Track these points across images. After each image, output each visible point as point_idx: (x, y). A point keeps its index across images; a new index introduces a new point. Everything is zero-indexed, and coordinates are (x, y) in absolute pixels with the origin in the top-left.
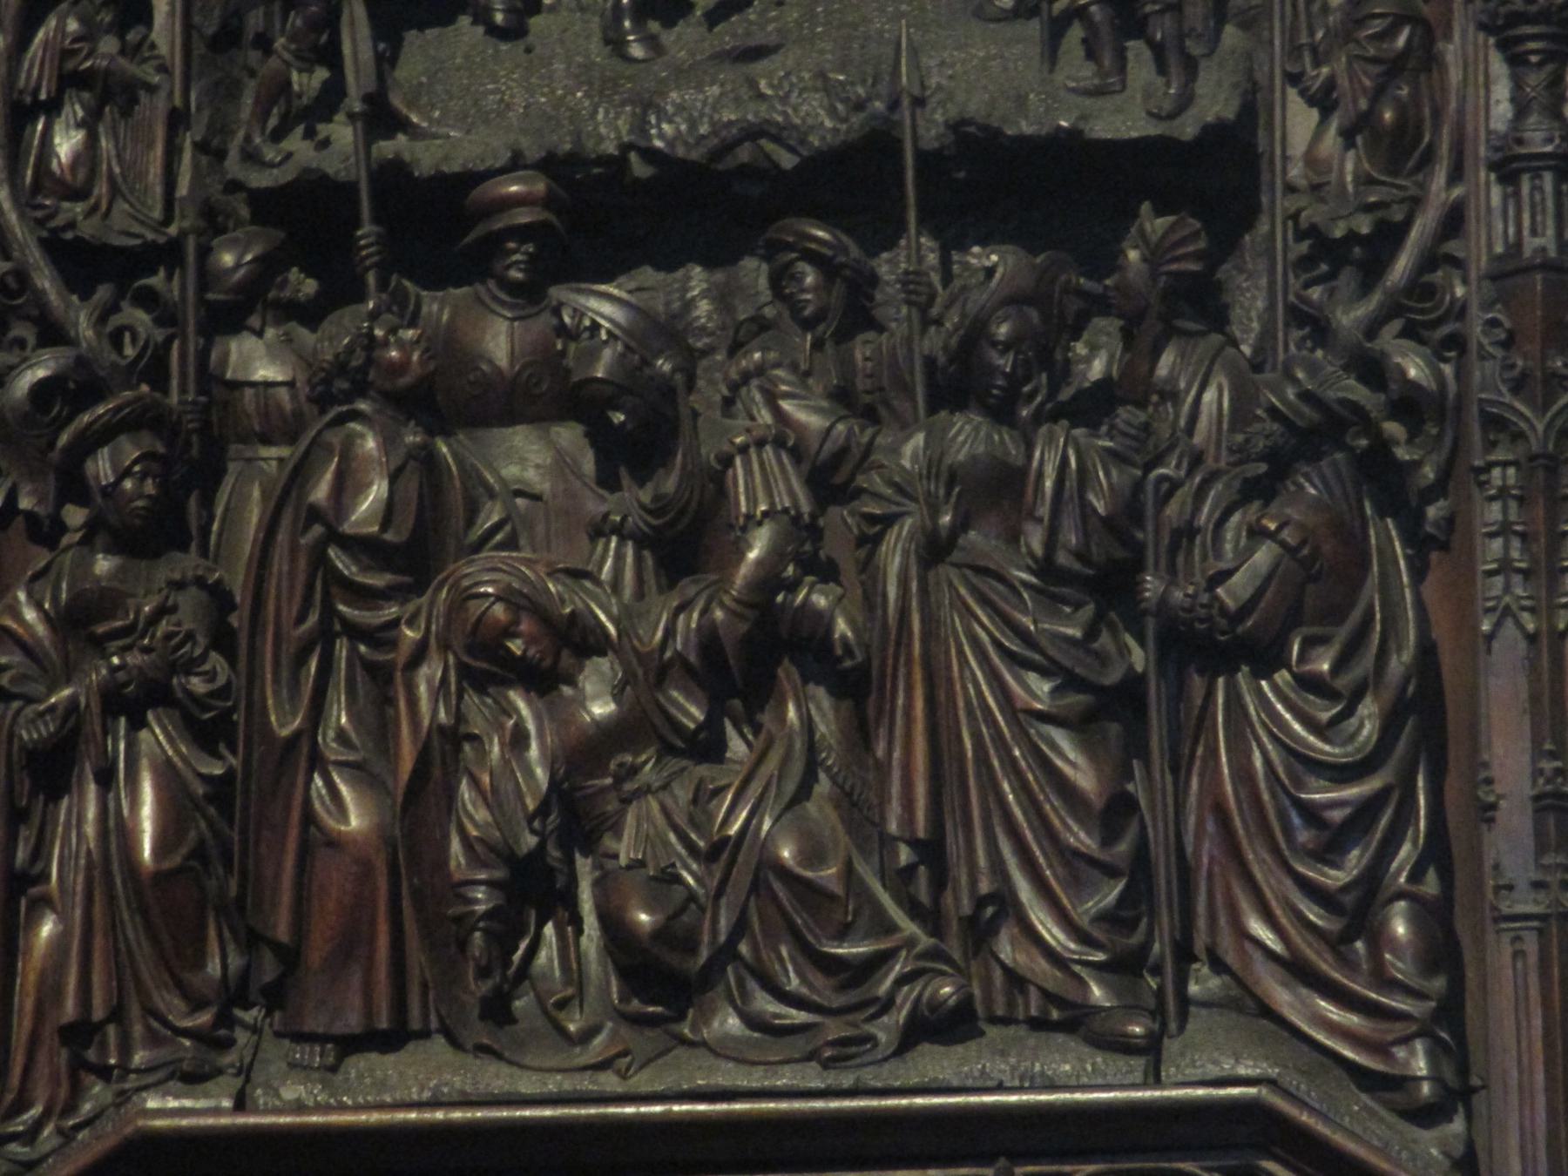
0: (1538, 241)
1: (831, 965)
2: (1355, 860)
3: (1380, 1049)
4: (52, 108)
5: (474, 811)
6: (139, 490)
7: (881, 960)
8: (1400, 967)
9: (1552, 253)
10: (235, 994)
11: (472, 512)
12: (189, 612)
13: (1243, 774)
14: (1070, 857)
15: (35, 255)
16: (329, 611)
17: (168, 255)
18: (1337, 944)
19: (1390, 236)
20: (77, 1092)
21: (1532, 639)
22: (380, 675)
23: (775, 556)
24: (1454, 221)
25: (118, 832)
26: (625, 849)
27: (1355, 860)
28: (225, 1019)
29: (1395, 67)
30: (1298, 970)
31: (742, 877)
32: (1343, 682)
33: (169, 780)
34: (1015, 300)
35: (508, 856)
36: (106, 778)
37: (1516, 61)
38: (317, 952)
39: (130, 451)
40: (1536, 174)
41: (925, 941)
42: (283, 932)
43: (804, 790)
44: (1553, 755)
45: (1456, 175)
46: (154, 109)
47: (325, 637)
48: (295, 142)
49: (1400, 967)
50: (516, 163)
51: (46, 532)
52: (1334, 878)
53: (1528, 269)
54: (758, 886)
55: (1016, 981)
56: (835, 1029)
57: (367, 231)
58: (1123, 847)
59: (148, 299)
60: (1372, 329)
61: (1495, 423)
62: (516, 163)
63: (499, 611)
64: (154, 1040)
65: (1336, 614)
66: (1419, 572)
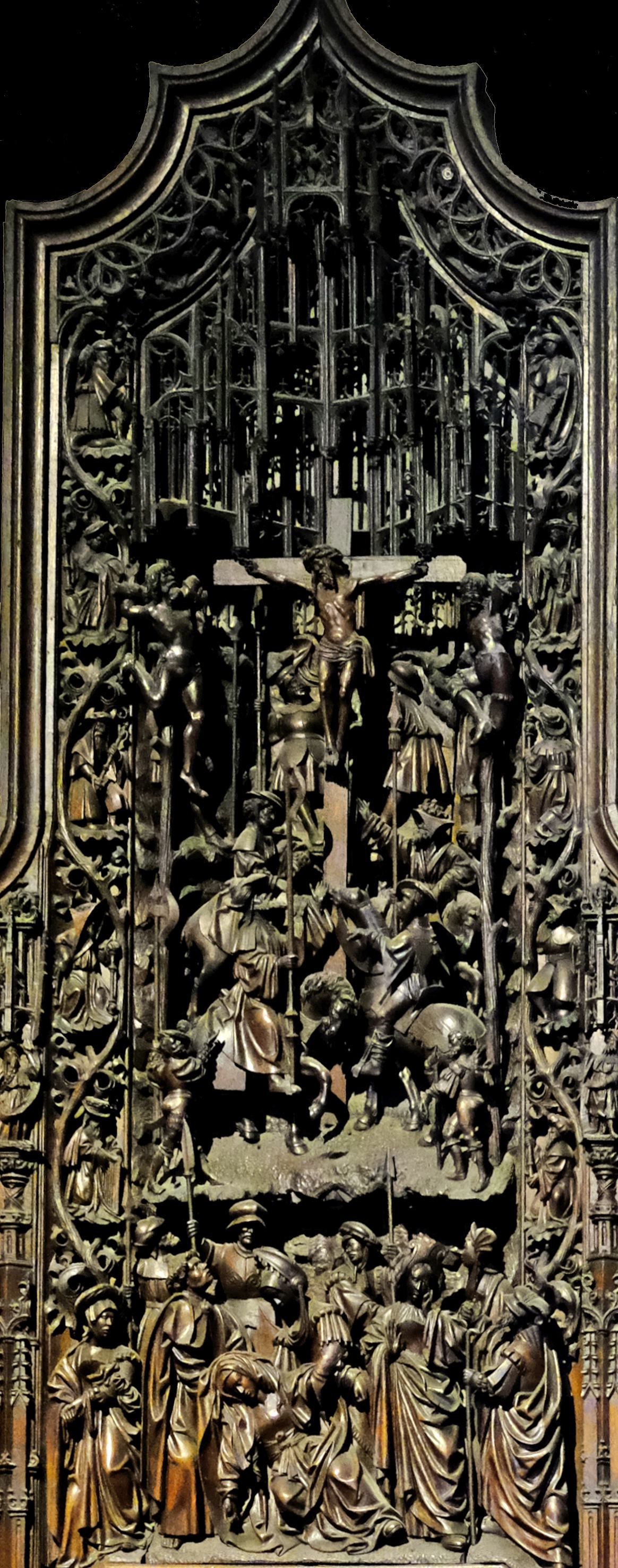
0: (604, 1248)
1: (352, 1515)
2: (538, 1480)
3: (545, 1552)
4: (77, 1168)
5: (225, 1452)
6: (106, 1323)
7: (370, 1514)
8: (553, 1523)
9: (609, 1253)
10: (143, 1518)
11: (229, 1334)
12: (124, 1371)
13: (500, 1448)
14: (437, 1477)
15: (70, 1227)
16: (173, 1374)
17: (119, 1228)
18: (532, 1511)
19: (555, 1242)
20: (86, 1552)
21: (598, 1399)
22: (193, 1396)
23: (335, 1359)
24: (579, 1237)
25: (97, 1456)
26: (280, 1467)
27: (538, 1480)
28: (141, 1527)
29: (559, 1176)
30: (517, 1521)
31: (321, 1482)
32: (533, 1414)
33: (118, 1434)
34: (422, 1261)
35: (238, 1469)
36: (94, 1434)
37: (599, 1177)
38: (171, 1502)
39: (102, 1306)
40: (604, 1221)
41: (388, 1506)
42: (157, 1495)
43: (345, 1448)
44: (604, 1444)
45: (580, 1219)
46: (115, 1170)
47: (173, 1382)
48: (168, 1185)
49: (553, 1523)
50: (247, 1196)
51: (76, 1334)
52: (529, 1487)
53: (600, 1258)
54: (326, 1485)
55: (419, 1523)
56: (353, 1539)
57: (191, 1222)
58: (458, 1473)
59: (113, 1244)
60: (551, 1277)
61: (589, 1317)
62: (247, 1196)
63: (234, 1376)
64: (114, 1535)
65: (532, 1387)
66: (565, 1370)
